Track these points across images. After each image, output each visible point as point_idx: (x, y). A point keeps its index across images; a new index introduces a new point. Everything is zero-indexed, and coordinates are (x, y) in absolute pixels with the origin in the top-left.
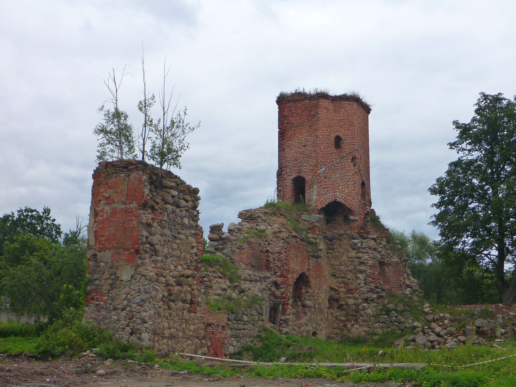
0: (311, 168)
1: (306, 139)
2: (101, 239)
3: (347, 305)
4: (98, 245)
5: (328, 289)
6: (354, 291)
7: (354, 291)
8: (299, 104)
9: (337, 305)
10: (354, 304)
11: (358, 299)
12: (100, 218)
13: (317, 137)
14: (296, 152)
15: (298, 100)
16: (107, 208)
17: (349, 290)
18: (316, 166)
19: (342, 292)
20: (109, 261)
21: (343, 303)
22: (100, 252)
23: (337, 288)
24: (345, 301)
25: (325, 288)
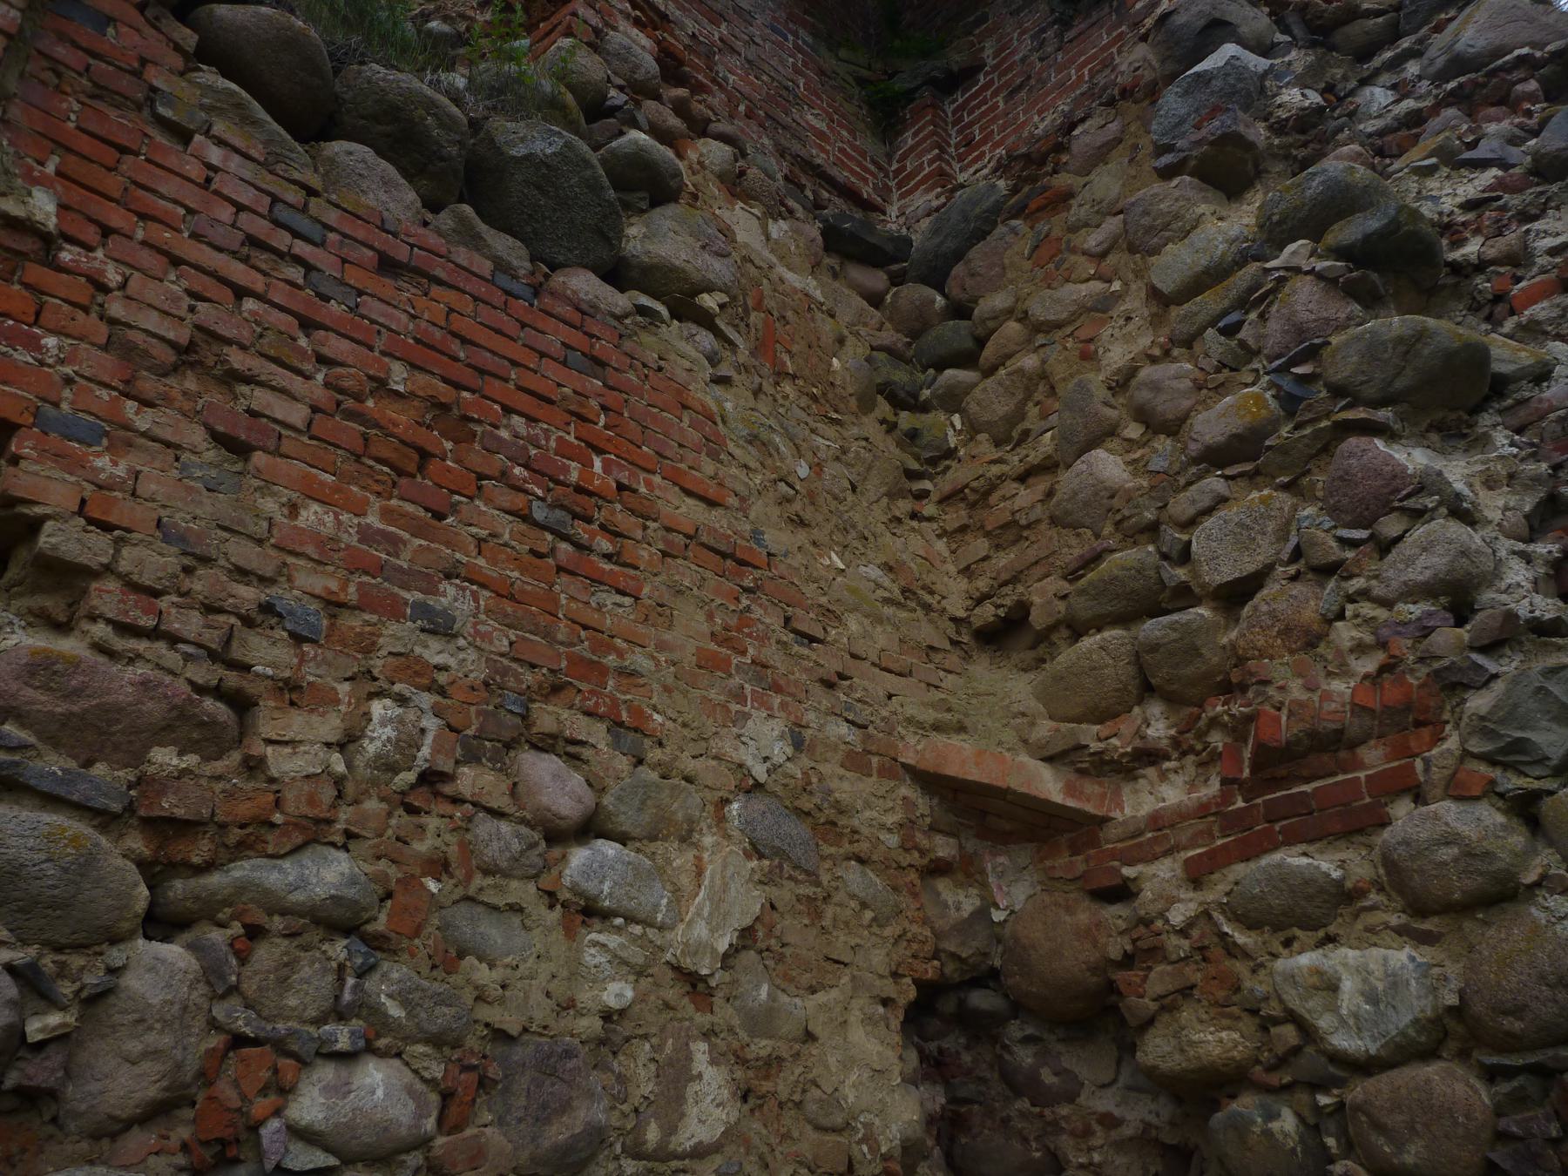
3: (1298, 1060)
5: (880, 810)
6: (1374, 758)
7: (1374, 758)
9: (1138, 1113)
10: (1451, 1032)
11: (1502, 895)
17: (1277, 764)
19: (1159, 833)
21: (1214, 1040)
23: (1049, 785)
24: (1232, 1003)
25: (762, 741)
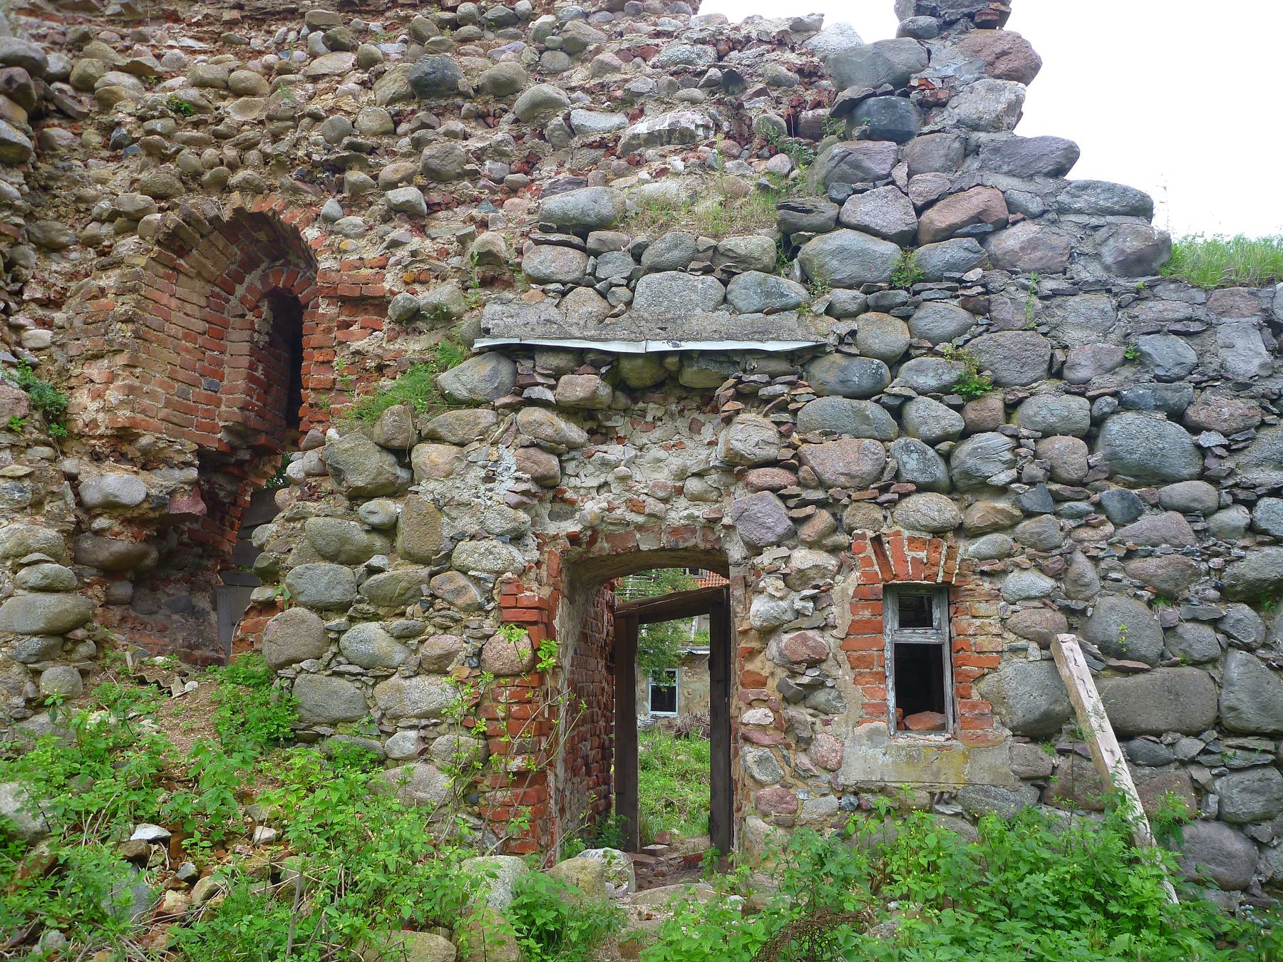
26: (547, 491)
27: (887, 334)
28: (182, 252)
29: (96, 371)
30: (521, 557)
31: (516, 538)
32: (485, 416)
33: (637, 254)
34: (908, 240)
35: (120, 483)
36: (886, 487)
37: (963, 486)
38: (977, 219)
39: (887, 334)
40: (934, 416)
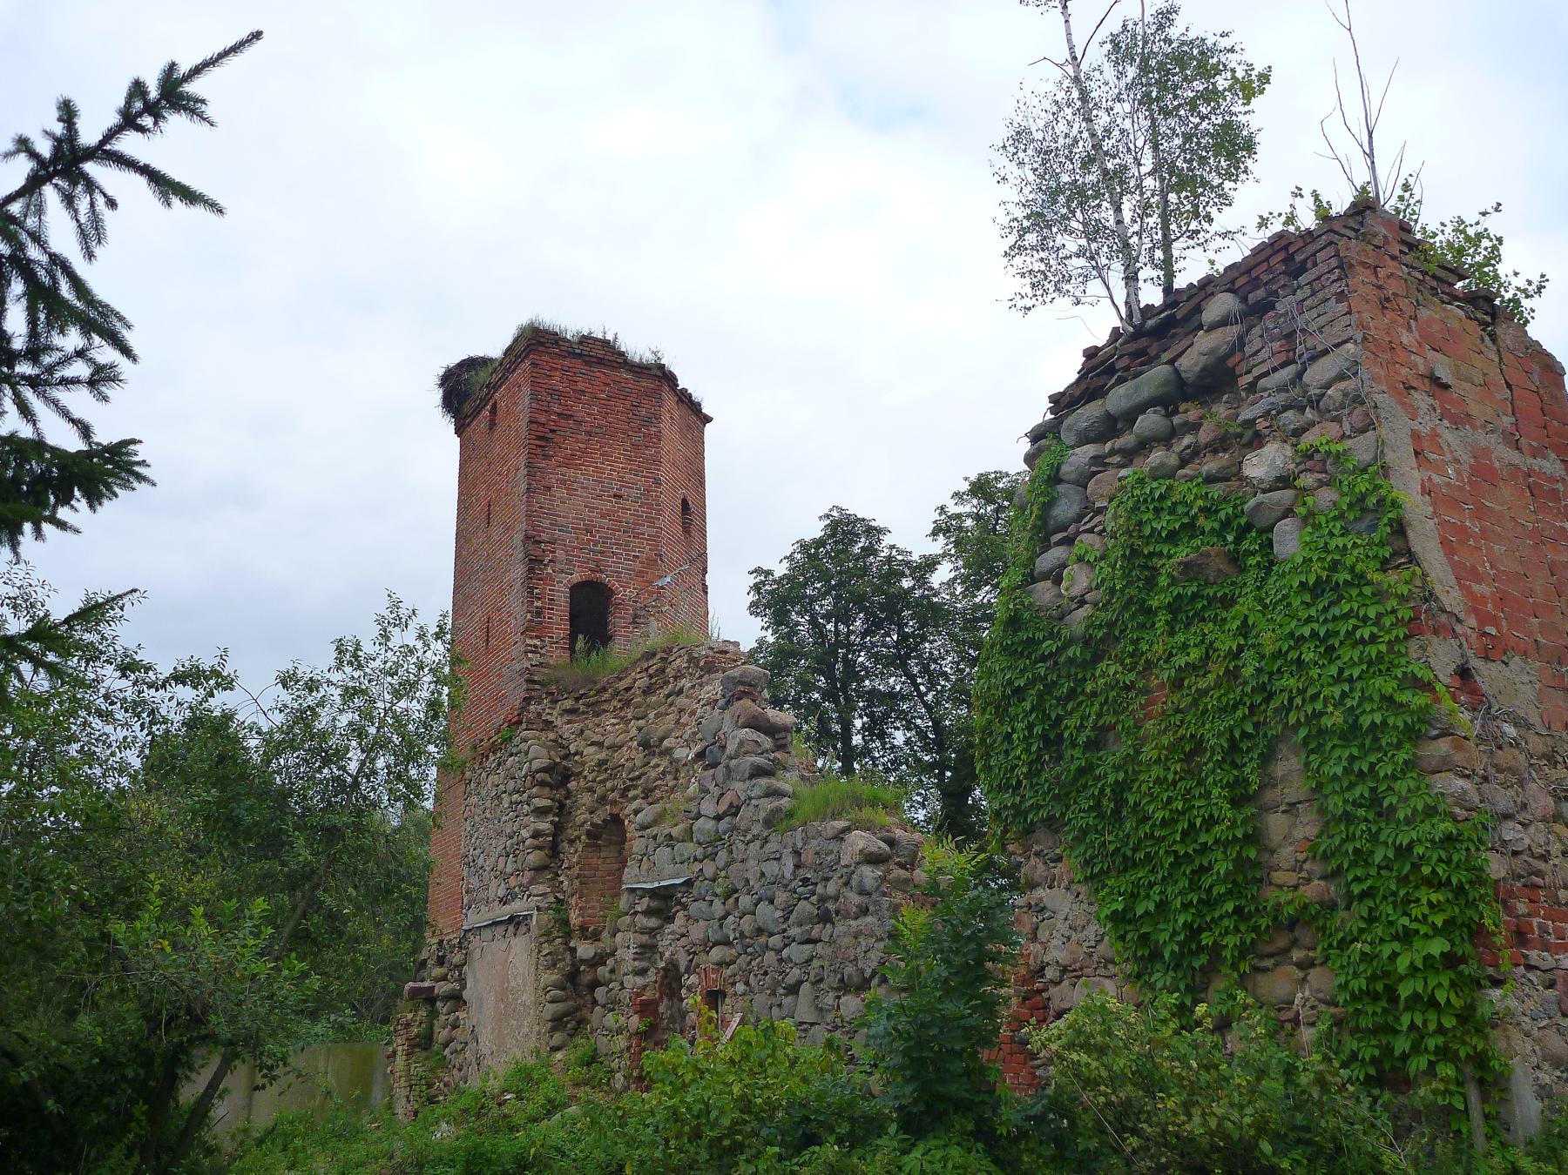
0: (637, 566)
1: (621, 479)
2: (1476, 587)
4: (1473, 622)
8: (601, 374)
12: (1436, 479)
13: (658, 483)
14: (591, 509)
15: (601, 361)
16: (1448, 436)
18: (652, 563)
20: (1534, 719)
22: (1487, 658)
26: (648, 950)
27: (709, 869)
28: (598, 837)
29: (573, 901)
30: (640, 981)
31: (642, 972)
32: (627, 919)
33: (655, 838)
34: (718, 818)
35: (585, 950)
36: (707, 945)
37: (727, 943)
38: (731, 805)
39: (709, 869)
40: (718, 908)
